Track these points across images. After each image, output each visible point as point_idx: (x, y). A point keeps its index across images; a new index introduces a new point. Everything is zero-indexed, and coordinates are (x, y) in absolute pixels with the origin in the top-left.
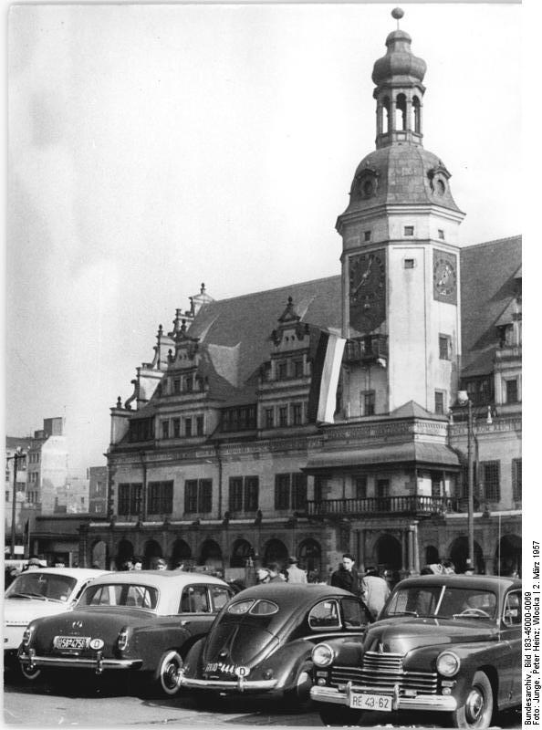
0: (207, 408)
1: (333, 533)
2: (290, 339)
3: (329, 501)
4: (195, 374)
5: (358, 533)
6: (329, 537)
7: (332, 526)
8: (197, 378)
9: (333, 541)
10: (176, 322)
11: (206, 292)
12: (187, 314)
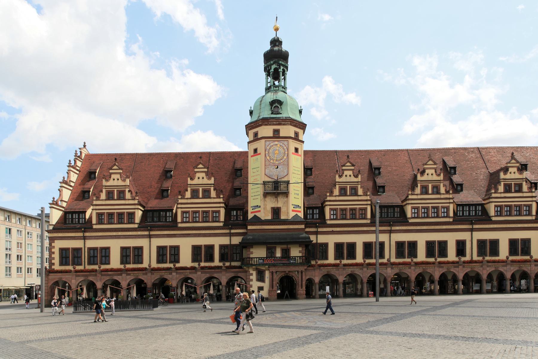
0: (138, 209)
1: (254, 273)
3: (252, 258)
4: (127, 190)
5: (272, 273)
6: (252, 274)
7: (254, 270)
8: (129, 191)
9: (254, 277)
10: (75, 161)
11: (86, 147)
12: (79, 157)
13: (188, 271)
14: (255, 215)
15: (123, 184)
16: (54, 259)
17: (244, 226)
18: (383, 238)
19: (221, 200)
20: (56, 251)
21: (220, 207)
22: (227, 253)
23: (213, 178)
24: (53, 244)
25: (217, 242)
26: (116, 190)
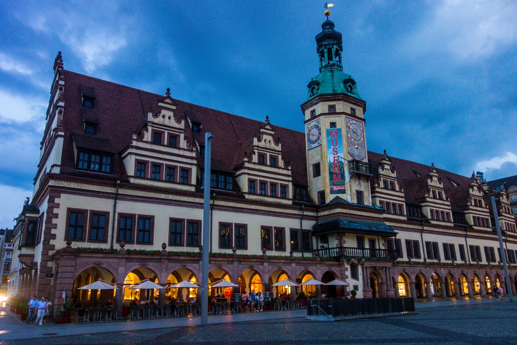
1: (348, 267)
2: (267, 141)
8: (185, 138)
13: (283, 261)
14: (337, 198)
15: (177, 125)
16: (55, 226)
17: (317, 208)
18: (415, 236)
19: (289, 173)
20: (62, 213)
21: (289, 181)
22: (301, 239)
23: (280, 145)
24: (57, 200)
25: (288, 224)
26: (166, 132)
